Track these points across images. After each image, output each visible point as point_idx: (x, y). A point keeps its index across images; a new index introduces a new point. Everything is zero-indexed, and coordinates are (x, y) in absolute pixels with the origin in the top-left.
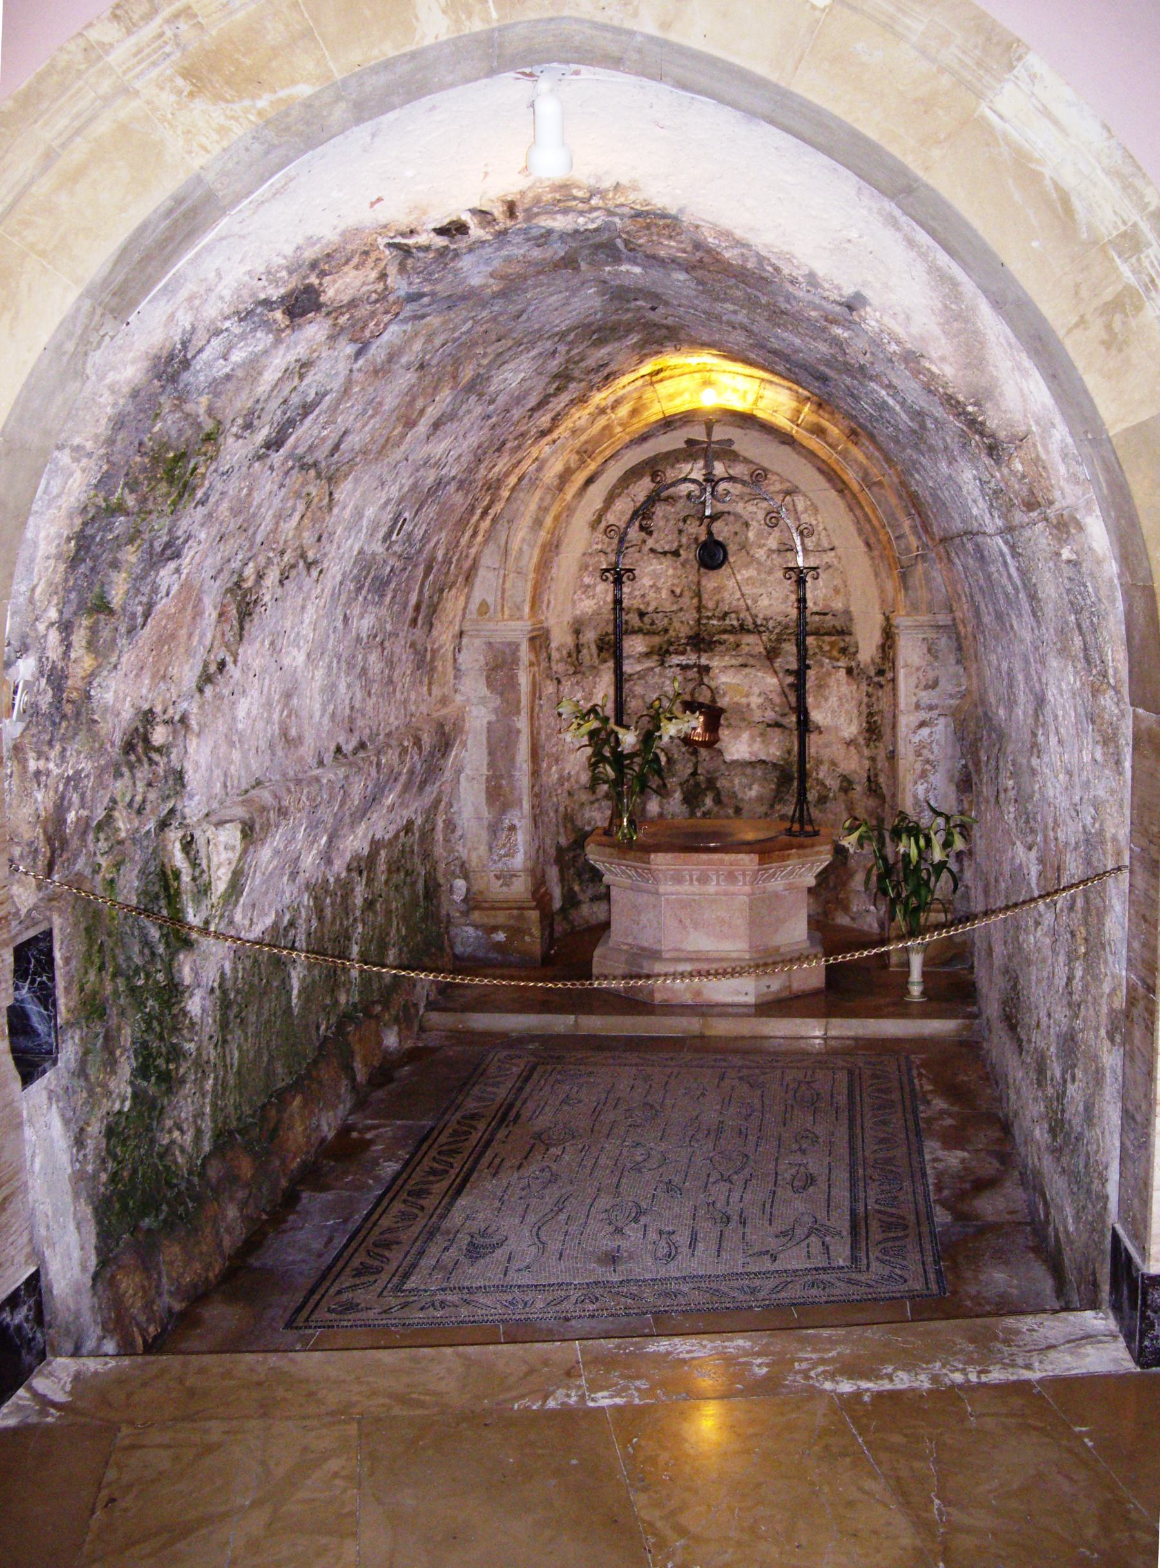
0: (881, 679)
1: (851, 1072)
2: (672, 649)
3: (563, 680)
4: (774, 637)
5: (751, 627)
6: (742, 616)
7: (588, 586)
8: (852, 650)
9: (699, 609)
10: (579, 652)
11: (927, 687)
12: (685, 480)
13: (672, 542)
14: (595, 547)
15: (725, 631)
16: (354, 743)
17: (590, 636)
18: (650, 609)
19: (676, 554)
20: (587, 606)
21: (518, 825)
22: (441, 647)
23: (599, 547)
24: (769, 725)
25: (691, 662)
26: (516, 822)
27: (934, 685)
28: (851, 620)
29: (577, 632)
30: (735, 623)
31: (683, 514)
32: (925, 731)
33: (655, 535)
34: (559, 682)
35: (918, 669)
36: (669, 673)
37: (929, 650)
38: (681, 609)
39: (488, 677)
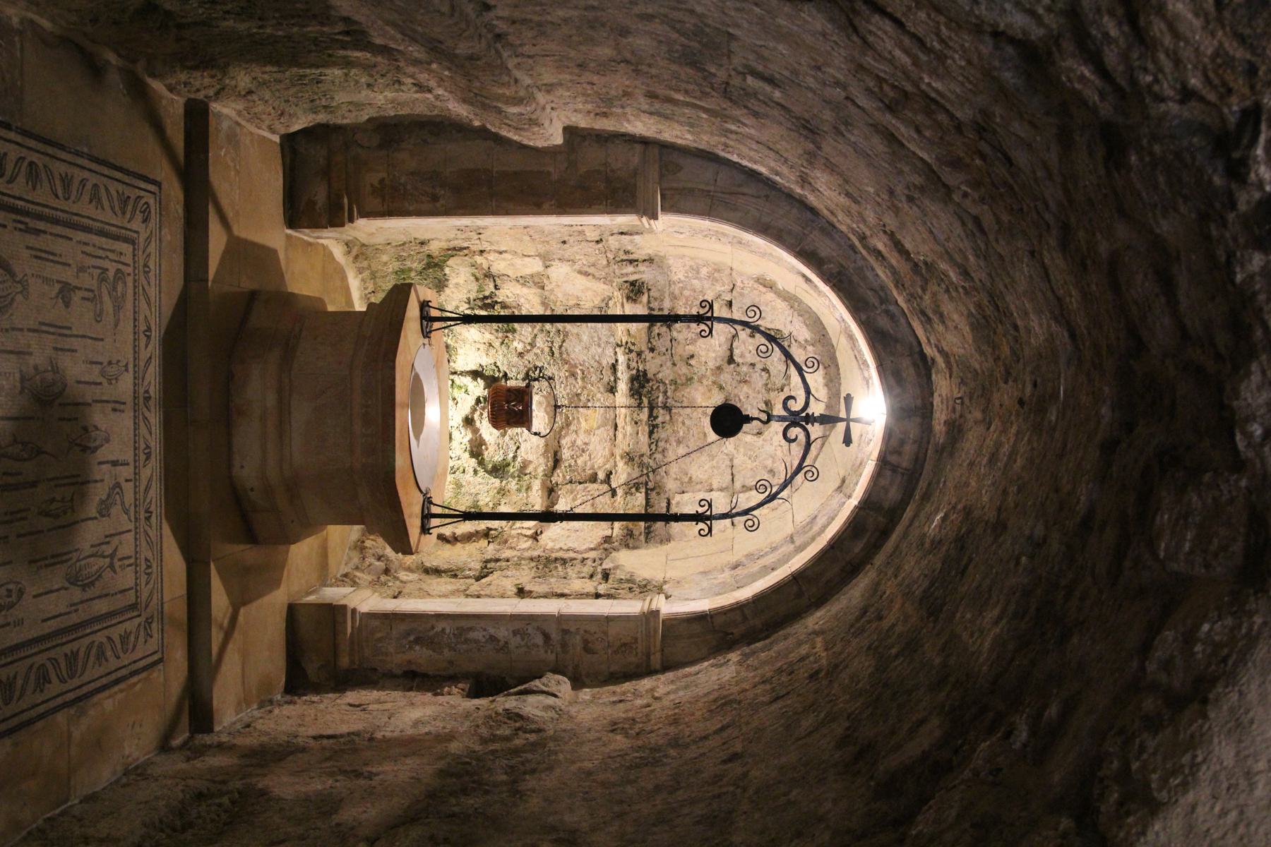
0: (600, 576)
1: (133, 607)
2: (633, 355)
3: (600, 245)
4: (646, 459)
5: (655, 436)
6: (667, 426)
7: (698, 273)
8: (631, 542)
9: (674, 382)
10: (631, 262)
11: (586, 642)
12: (808, 392)
13: (742, 356)
14: (739, 281)
15: (651, 408)
16: (502, 27)
17: (645, 274)
18: (675, 334)
19: (731, 360)
20: (678, 273)
21: (438, 205)
22: (628, 121)
23: (739, 284)
24: (556, 453)
25: (619, 374)
26: (442, 202)
27: (587, 648)
28: (661, 542)
29: (650, 260)
30: (660, 420)
31: (771, 369)
32: (539, 640)
33: (750, 340)
34: (597, 242)
35: (606, 633)
36: (610, 351)
37: (624, 645)
38: (674, 364)
39: (598, 172)
